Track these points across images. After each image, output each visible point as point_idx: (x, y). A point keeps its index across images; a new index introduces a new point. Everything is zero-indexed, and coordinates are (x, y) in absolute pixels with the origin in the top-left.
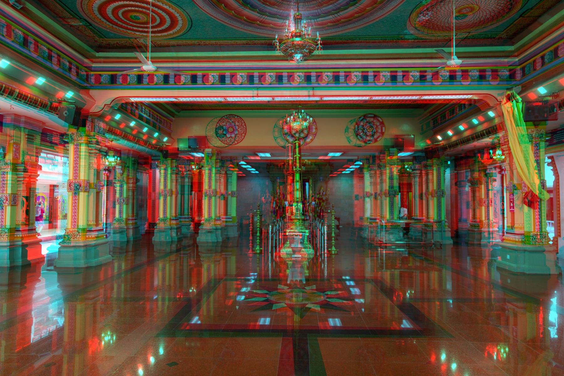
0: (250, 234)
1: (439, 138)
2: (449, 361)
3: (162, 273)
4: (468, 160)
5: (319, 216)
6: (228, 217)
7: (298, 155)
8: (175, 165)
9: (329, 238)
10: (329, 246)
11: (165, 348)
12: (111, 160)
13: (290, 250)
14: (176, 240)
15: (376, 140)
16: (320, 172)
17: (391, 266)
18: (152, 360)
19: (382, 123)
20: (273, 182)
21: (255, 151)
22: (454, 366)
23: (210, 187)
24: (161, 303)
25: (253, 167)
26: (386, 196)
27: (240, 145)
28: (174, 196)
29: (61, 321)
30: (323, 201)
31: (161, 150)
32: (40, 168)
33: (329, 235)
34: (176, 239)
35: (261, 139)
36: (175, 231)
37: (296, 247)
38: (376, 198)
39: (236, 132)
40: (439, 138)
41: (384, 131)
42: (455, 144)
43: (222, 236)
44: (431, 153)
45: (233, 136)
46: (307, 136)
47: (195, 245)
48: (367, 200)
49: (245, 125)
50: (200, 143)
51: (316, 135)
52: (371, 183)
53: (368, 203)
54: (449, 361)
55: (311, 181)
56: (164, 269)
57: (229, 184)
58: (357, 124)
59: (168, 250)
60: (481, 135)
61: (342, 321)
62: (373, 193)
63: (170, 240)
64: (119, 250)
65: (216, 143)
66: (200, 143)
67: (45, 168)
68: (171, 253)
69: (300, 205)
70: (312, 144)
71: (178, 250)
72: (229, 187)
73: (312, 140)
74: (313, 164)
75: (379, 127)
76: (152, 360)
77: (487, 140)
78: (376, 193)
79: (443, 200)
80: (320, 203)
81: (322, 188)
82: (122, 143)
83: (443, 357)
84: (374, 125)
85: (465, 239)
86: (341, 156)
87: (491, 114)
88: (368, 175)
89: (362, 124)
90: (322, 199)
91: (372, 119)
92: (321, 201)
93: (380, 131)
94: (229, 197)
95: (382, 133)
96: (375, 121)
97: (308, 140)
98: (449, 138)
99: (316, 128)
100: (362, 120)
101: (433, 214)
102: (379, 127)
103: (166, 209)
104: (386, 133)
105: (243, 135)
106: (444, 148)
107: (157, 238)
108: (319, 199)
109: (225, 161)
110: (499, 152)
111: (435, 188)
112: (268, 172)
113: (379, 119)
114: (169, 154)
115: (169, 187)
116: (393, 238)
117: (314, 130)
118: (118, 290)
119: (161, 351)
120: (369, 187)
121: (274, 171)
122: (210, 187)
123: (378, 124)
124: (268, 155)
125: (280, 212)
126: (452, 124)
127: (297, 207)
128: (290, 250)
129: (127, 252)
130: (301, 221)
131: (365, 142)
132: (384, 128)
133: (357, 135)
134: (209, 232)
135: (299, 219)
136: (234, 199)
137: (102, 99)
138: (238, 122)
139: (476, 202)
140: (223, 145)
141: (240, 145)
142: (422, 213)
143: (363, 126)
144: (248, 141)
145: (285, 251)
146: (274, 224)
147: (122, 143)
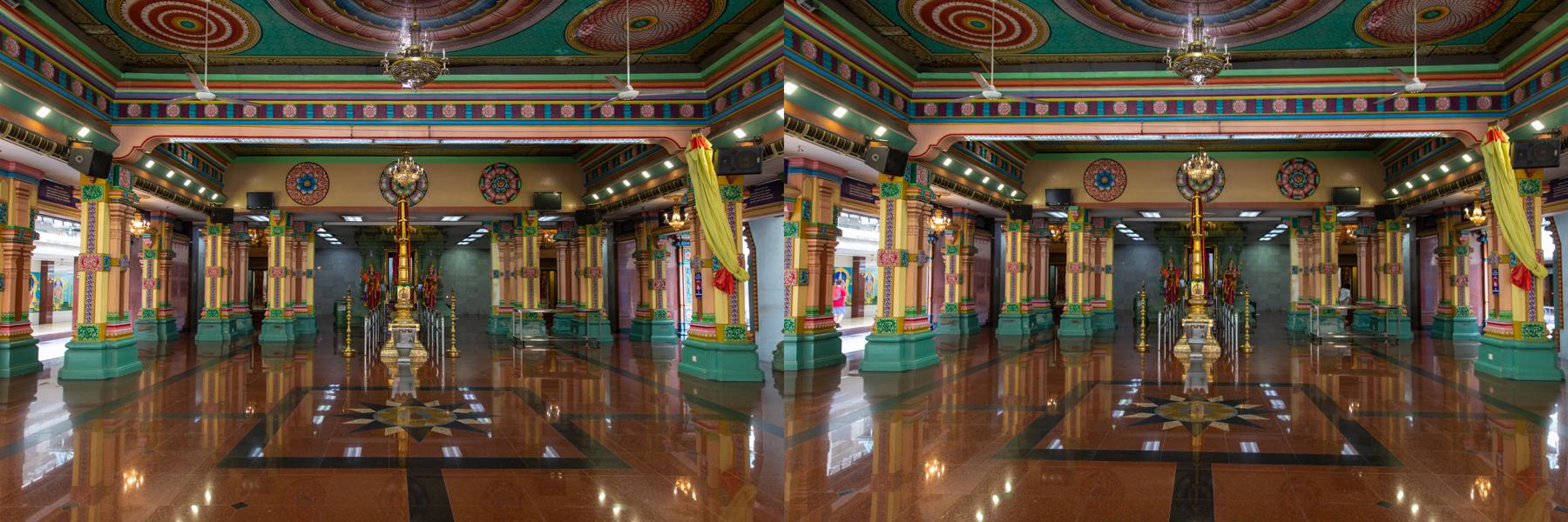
0: (336, 328)
1: (596, 197)
2: (610, 503)
3: (210, 386)
4: (637, 226)
7: (403, 219)
8: (228, 231)
9: (448, 335)
10: (448, 345)
11: (215, 494)
12: (138, 225)
13: (395, 352)
16: (433, 242)
17: (531, 373)
18: (195, 509)
21: (341, 213)
22: (617, 510)
24: (210, 429)
29: (62, 457)
31: (208, 211)
32: (37, 236)
33: (448, 329)
34: (228, 337)
35: (353, 196)
37: (402, 348)
40: (596, 197)
42: (617, 206)
44: (585, 217)
46: (414, 193)
47: (257, 345)
50: (264, 201)
54: (610, 503)
56: (212, 381)
59: (218, 353)
60: (654, 193)
61: (462, 451)
64: (149, 354)
66: (264, 201)
67: (44, 237)
71: (232, 354)
76: (195, 509)
77: (661, 200)
79: (600, 282)
82: (153, 200)
83: (602, 497)
85: (632, 334)
87: (669, 165)
98: (609, 197)
101: (587, 300)
103: (215, 295)
106: (602, 211)
107: (203, 335)
109: (299, 227)
110: (676, 216)
114: (223, 216)
116: (532, 335)
118: (146, 410)
119: (208, 497)
121: (371, 242)
124: (359, 219)
126: (613, 179)
127: (404, 291)
128: (395, 352)
129: (158, 357)
137: (132, 139)
139: (647, 284)
140: (294, 204)
144: (332, 200)
145: (388, 353)
146: (370, 316)
147: (153, 200)
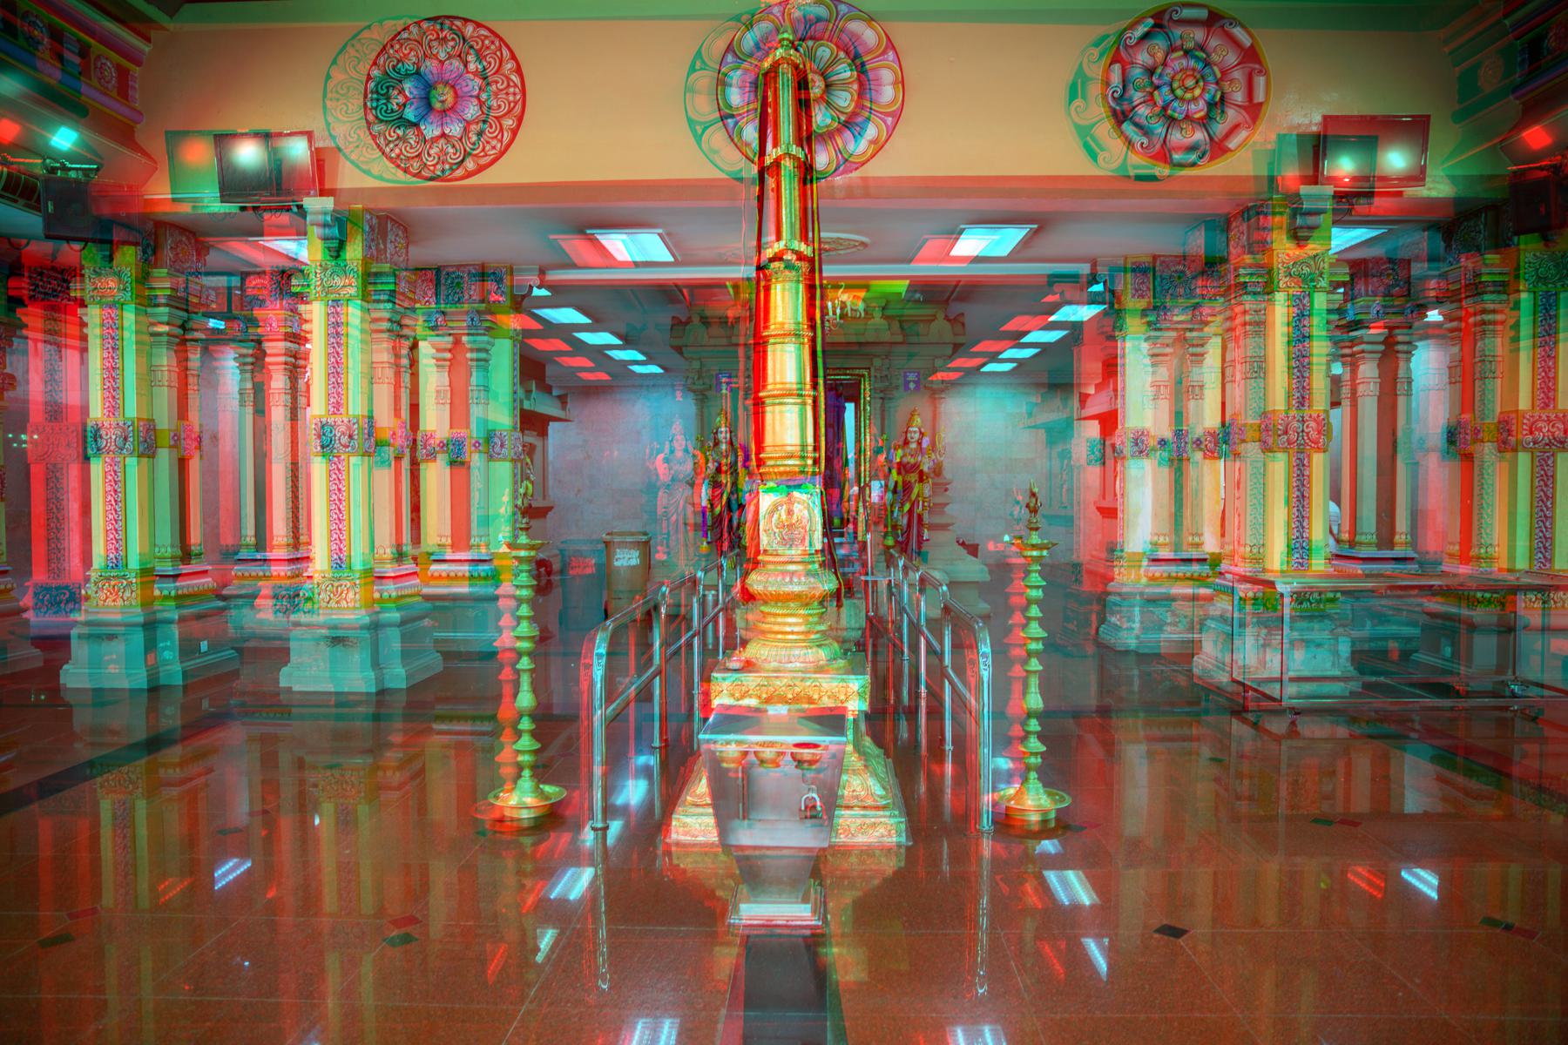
5: (903, 547)
14: (178, 681)
15: (1218, 148)
19: (1250, 56)
20: (703, 396)
25: (628, 342)
26: (1267, 449)
27: (494, 176)
28: (164, 458)
30: (922, 478)
36: (175, 631)
39: (472, 111)
41: (1260, 96)
43: (406, 656)
45: (455, 129)
49: (519, 71)
51: (897, 116)
52: (1156, 386)
53: (1143, 487)
55: (866, 388)
58: (1116, 59)
62: (1168, 434)
63: (140, 680)
65: (367, 171)
68: (154, 744)
69: (808, 506)
70: (878, 169)
72: (476, 411)
73: (878, 146)
74: (877, 313)
75: (1237, 74)
78: (1179, 434)
80: (908, 487)
81: (918, 420)
84: (1207, 63)
86: (1011, 258)
89: (1143, 57)
90: (915, 467)
91: (1199, 34)
92: (913, 477)
93: (1239, 97)
94: (477, 460)
95: (1253, 110)
96: (1214, 42)
97: (858, 146)
99: (901, 82)
100: (1146, 36)
102: (1237, 74)
104: (1268, 111)
105: (509, 123)
108: (903, 468)
111: (1524, 403)
112: (679, 349)
113: (1238, 32)
115: (131, 410)
117: (888, 93)
120: (1149, 405)
123: (1232, 58)
125: (727, 530)
130: (815, 610)
131: (1163, 155)
132: (1260, 81)
133: (1121, 116)
134: (337, 641)
135: (802, 599)
136: (503, 471)
138: (480, 57)
141: (494, 176)
142: (1393, 532)
143: (1150, 71)
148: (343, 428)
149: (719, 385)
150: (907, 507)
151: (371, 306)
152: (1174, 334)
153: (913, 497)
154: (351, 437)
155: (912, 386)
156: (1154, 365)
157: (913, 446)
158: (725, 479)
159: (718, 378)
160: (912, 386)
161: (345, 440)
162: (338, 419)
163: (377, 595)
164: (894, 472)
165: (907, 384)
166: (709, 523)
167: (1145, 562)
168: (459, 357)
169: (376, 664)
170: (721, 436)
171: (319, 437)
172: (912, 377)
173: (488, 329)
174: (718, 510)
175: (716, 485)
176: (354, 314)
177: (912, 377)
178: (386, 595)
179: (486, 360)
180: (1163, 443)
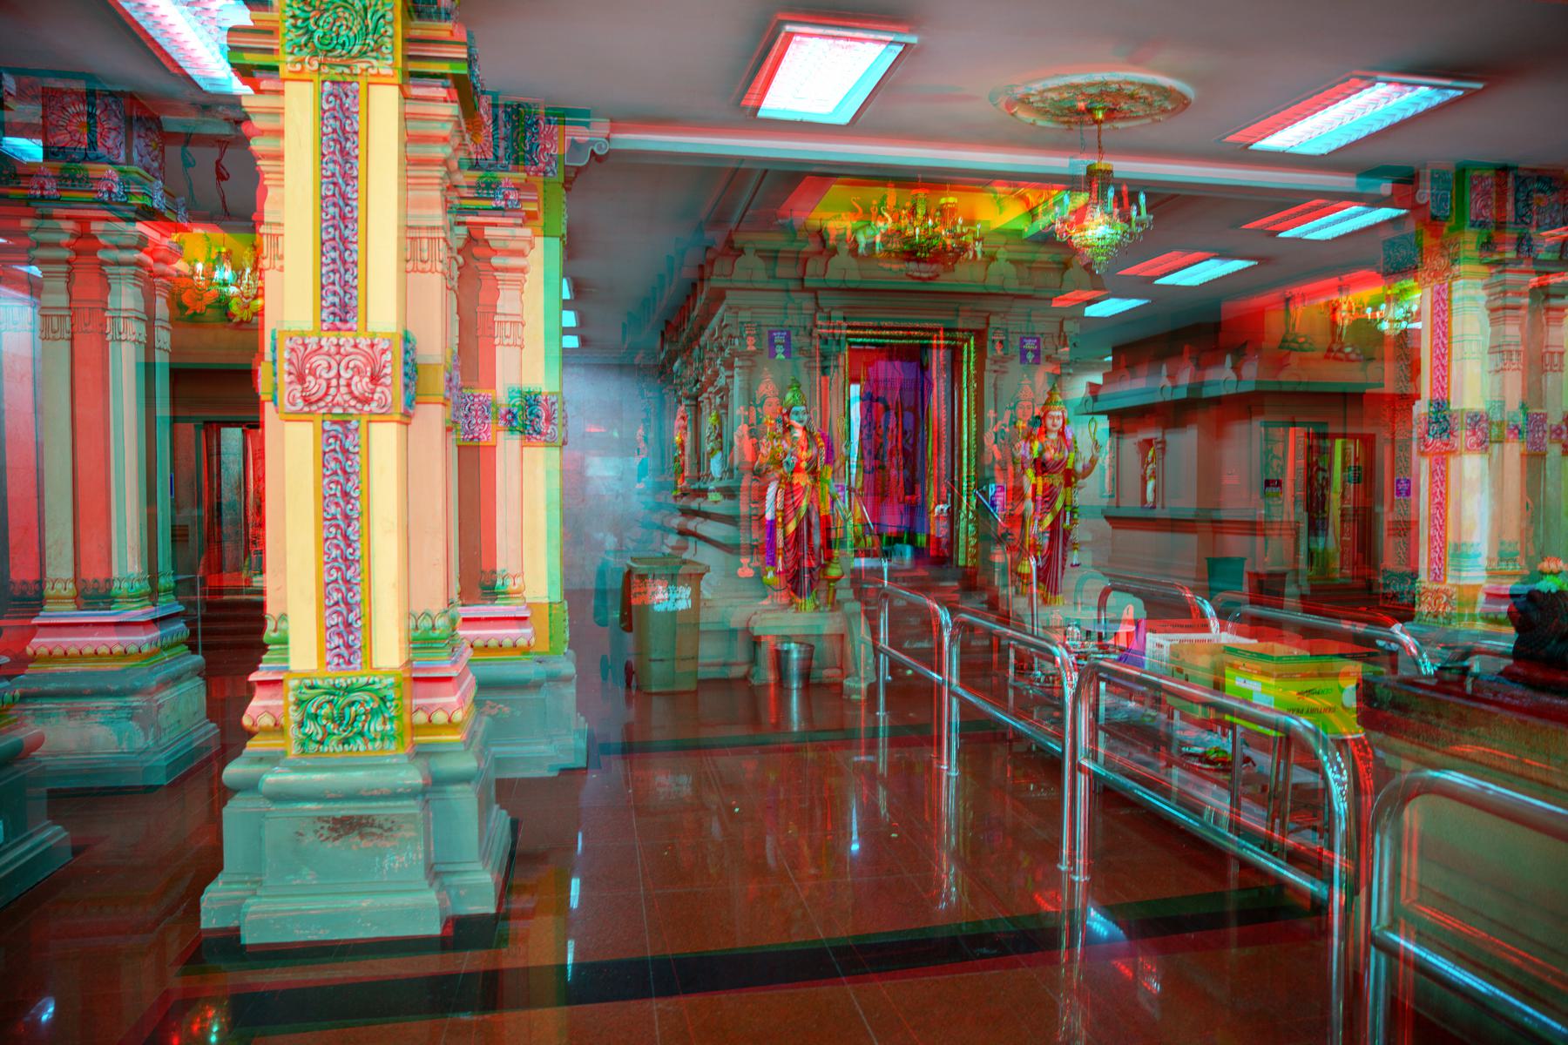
6: (499, 609)
23: (341, 305)
38: (1534, 459)
48: (1471, 468)
57: (502, 332)
62: (1520, 420)
78: (1536, 422)
88: (1482, 295)
94: (507, 446)
122: (341, 305)
134: (346, 826)
148: (358, 361)
149: (772, 344)
150: (1048, 520)
151: (412, 107)
152: (1534, 280)
153: (1059, 506)
154: (375, 379)
155: (1030, 356)
156: (1493, 322)
157: (1053, 436)
158: (803, 480)
159: (771, 339)
160: (1030, 356)
161: (361, 385)
162: (346, 340)
163: (421, 718)
164: (1030, 472)
165: (1024, 353)
166: (780, 543)
167: (1482, 597)
168: (473, 264)
169: (435, 873)
170: (794, 420)
171: (301, 379)
172: (1030, 345)
173: (531, 217)
174: (792, 527)
175: (790, 490)
176: (383, 109)
177: (1030, 345)
178: (440, 717)
179: (522, 270)
180: (1516, 431)
